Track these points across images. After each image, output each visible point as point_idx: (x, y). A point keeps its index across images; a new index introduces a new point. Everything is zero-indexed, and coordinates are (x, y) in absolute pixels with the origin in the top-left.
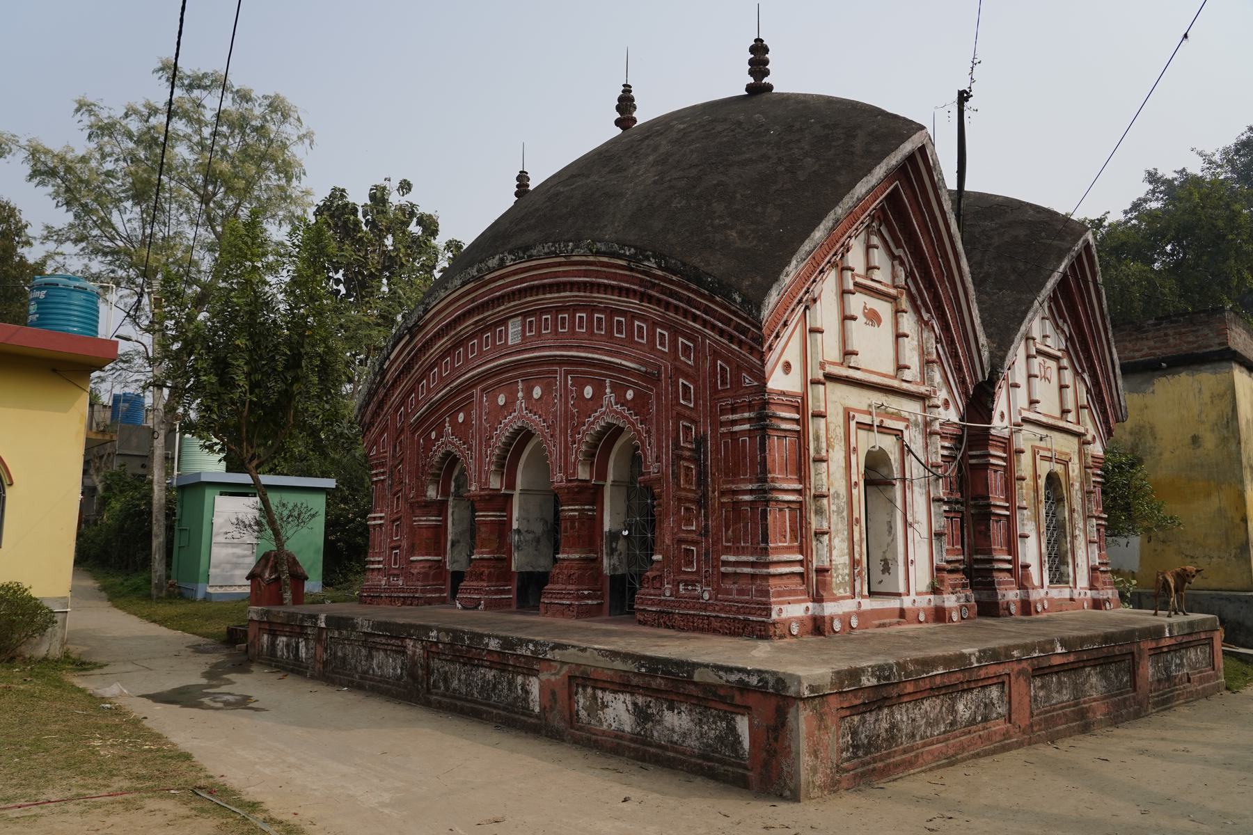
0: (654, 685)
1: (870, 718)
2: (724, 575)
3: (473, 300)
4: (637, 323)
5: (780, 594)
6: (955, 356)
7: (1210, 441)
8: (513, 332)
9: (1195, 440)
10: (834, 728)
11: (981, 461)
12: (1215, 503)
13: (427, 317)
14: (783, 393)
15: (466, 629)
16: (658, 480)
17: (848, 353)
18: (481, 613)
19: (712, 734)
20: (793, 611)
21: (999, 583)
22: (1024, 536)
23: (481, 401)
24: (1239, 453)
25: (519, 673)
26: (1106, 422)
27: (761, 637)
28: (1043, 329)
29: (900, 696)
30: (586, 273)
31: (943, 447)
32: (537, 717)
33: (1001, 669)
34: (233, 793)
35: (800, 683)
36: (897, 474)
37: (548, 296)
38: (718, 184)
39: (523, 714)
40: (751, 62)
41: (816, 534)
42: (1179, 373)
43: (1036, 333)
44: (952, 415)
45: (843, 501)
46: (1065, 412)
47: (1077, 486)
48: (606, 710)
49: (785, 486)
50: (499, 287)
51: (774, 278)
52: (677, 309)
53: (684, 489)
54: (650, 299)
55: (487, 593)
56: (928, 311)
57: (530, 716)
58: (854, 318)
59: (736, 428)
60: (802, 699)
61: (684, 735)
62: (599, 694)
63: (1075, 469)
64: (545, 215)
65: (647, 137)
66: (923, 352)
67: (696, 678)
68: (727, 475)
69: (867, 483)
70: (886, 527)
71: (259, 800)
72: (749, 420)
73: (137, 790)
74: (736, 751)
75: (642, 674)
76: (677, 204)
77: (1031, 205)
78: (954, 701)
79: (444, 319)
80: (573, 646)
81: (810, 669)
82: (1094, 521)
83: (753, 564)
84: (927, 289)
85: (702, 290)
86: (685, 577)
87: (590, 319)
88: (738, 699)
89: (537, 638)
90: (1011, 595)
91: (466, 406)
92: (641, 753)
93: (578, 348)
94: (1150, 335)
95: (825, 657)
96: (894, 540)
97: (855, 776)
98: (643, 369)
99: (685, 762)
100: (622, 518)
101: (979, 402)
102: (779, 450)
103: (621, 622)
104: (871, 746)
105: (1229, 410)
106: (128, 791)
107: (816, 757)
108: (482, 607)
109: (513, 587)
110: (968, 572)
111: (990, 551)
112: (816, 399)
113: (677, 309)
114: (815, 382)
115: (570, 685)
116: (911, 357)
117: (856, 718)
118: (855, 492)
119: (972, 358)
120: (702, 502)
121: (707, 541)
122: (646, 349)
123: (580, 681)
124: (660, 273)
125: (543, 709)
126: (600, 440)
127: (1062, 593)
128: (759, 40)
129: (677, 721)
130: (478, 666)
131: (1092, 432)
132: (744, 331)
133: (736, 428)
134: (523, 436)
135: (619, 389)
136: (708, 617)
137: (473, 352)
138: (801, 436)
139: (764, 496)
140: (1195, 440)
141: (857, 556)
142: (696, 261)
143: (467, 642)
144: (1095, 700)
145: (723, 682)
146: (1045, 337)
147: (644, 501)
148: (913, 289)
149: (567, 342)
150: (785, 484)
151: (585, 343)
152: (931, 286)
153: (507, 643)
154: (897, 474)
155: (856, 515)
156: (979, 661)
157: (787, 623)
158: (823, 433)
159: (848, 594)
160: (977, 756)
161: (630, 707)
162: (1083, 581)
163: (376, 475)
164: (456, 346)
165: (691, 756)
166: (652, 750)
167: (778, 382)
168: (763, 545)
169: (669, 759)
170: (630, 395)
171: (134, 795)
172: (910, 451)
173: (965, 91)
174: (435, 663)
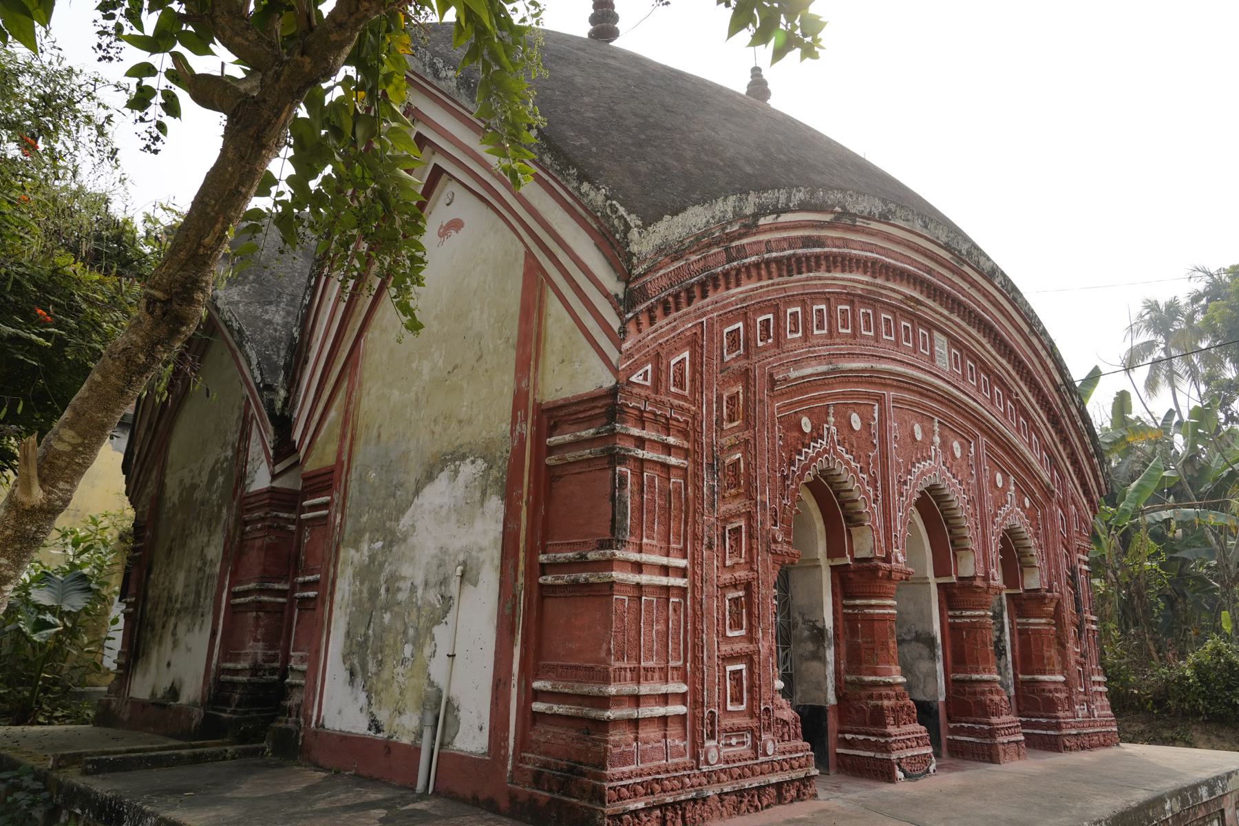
13: (874, 225)
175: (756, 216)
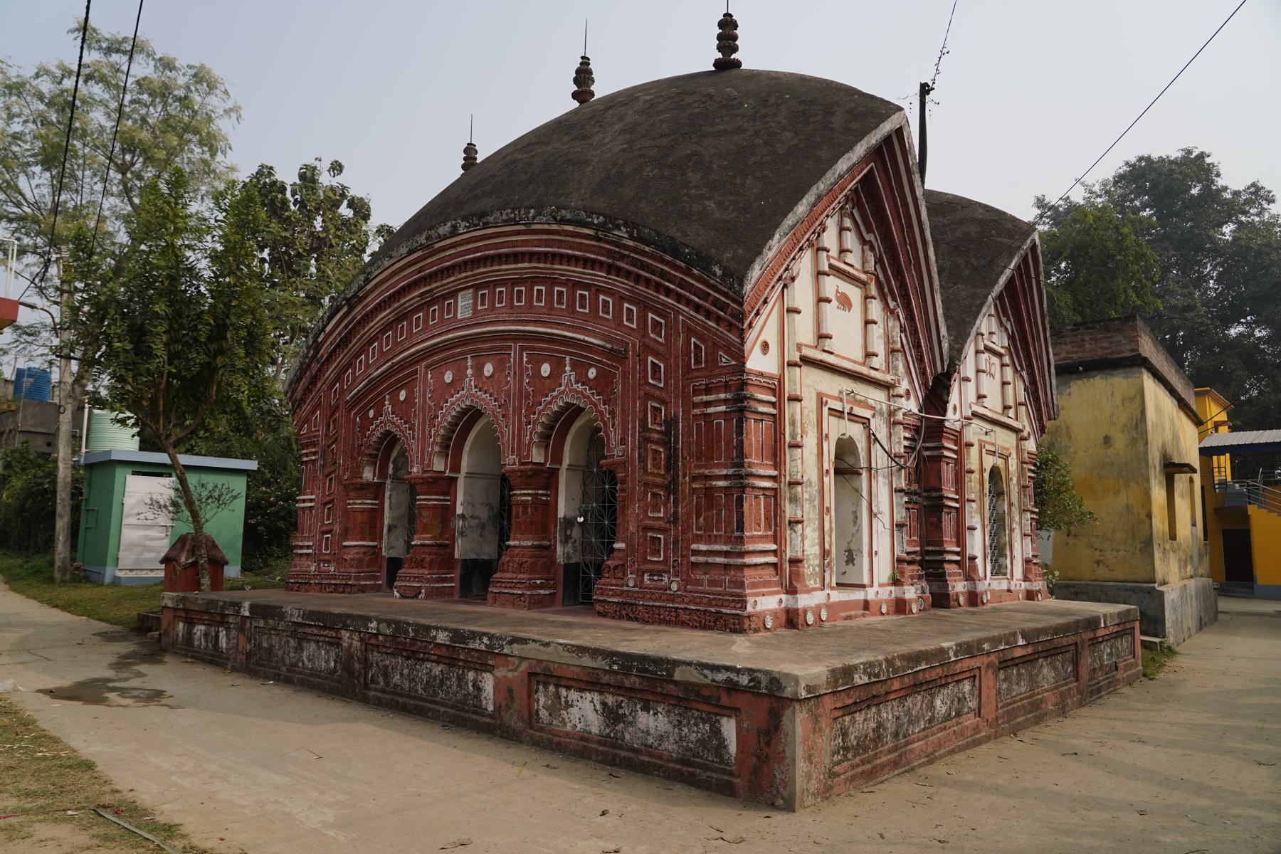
0: (627, 683)
1: (859, 717)
2: (695, 565)
3: (420, 270)
4: (601, 297)
5: (754, 586)
6: (917, 346)
7: (1120, 442)
8: (464, 305)
9: (1107, 440)
10: (827, 731)
11: (935, 453)
12: (1122, 500)
13: (368, 287)
14: (761, 374)
15: (411, 620)
16: (623, 464)
17: (822, 337)
18: (421, 602)
19: (693, 737)
20: (766, 603)
21: (950, 575)
22: (972, 529)
23: (425, 378)
24: (1146, 453)
25: (470, 669)
26: (1040, 419)
27: (734, 631)
28: (990, 326)
29: (887, 693)
30: (547, 243)
31: (905, 438)
32: (491, 716)
33: (974, 663)
34: (146, 812)
35: (797, 683)
36: (863, 464)
37: (504, 267)
38: (692, 155)
39: (475, 713)
40: (719, 37)
41: (790, 523)
42: (1093, 377)
43: (984, 330)
44: (912, 405)
45: (814, 489)
46: (1006, 408)
47: (1015, 480)
48: (570, 710)
49: (761, 472)
50: (449, 257)
51: (757, 251)
52: (648, 282)
53: (652, 474)
54: (619, 271)
55: (429, 581)
56: (894, 299)
57: (482, 715)
58: (828, 301)
59: (711, 410)
60: (799, 700)
61: (661, 738)
62: (563, 692)
63: (1013, 462)
64: (492, 190)
65: (611, 108)
66: (888, 340)
67: (678, 676)
68: (699, 459)
69: (838, 472)
70: (851, 517)
71: (177, 821)
72: (725, 401)
73: (25, 812)
74: (720, 756)
75: (614, 672)
76: (648, 172)
77: (980, 204)
78: (932, 696)
79: (387, 290)
80: (534, 641)
81: (806, 668)
82: (1029, 515)
83: (726, 554)
84: (894, 279)
85: (678, 262)
86: (650, 567)
87: (550, 293)
88: (725, 700)
89: (492, 631)
90: (958, 587)
91: (409, 383)
92: (612, 757)
93: (536, 322)
94: (1068, 340)
95: (812, 653)
96: (859, 530)
97: (846, 779)
98: (609, 346)
99: (661, 766)
100: (577, 504)
101: (936, 395)
102: (755, 433)
103: (577, 613)
104: (861, 747)
105: (1139, 412)
106: (14, 813)
107: (811, 762)
108: (422, 595)
109: (456, 574)
110: (922, 564)
111: (941, 543)
112: (792, 381)
113: (648, 282)
114: (792, 364)
115: (530, 683)
116: (878, 346)
117: (847, 719)
118: (826, 479)
119: (932, 349)
120: (671, 487)
121: (676, 529)
122: (612, 325)
123: (541, 678)
124: (631, 243)
125: (498, 708)
126: (557, 421)
127: (1000, 584)
128: (727, 15)
129: (652, 723)
130: (423, 660)
131: (1028, 429)
132: (723, 307)
133: (711, 410)
134: (471, 415)
135: (580, 368)
136: (676, 609)
137: (417, 326)
138: (777, 420)
139: (740, 482)
140: (1107, 440)
141: (827, 547)
142: (672, 231)
143: (412, 634)
144: (1047, 691)
145: (708, 681)
146: (991, 333)
147: (604, 488)
148: (881, 276)
149: (524, 317)
150: (760, 467)
151: (544, 318)
152: (898, 274)
153: (458, 636)
154: (863, 464)
155: (827, 504)
156: (956, 655)
157: (761, 616)
158: (798, 417)
159: (818, 585)
160: (952, 752)
161: (598, 707)
162: (1018, 573)
163: (307, 455)
164: (399, 319)
165: (668, 760)
166: (623, 753)
167: (758, 362)
168: (737, 534)
169: (642, 763)
170: (592, 373)
171: (22, 818)
172: (876, 439)
173: (926, 84)
174: (375, 657)
175: (315, 340)
